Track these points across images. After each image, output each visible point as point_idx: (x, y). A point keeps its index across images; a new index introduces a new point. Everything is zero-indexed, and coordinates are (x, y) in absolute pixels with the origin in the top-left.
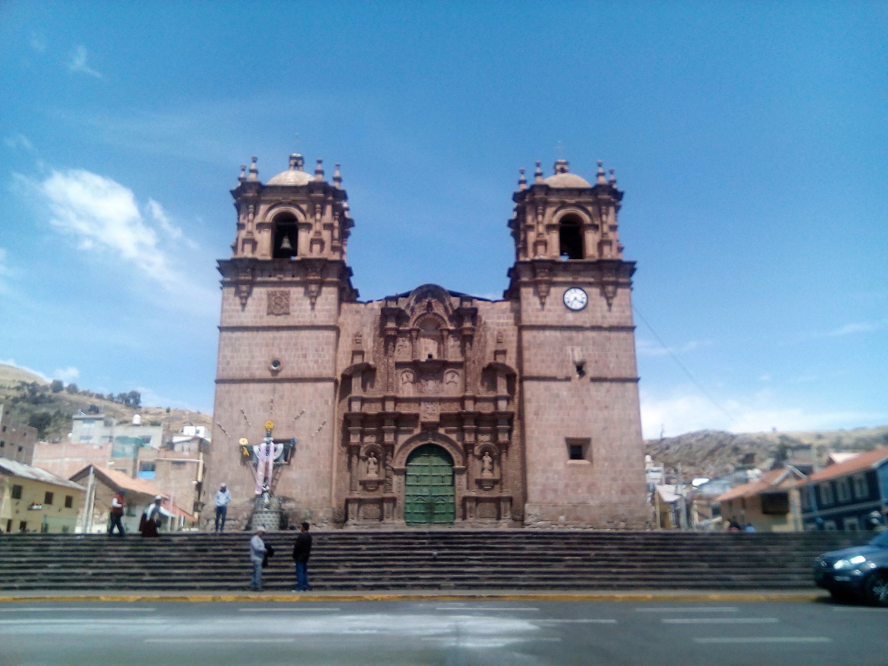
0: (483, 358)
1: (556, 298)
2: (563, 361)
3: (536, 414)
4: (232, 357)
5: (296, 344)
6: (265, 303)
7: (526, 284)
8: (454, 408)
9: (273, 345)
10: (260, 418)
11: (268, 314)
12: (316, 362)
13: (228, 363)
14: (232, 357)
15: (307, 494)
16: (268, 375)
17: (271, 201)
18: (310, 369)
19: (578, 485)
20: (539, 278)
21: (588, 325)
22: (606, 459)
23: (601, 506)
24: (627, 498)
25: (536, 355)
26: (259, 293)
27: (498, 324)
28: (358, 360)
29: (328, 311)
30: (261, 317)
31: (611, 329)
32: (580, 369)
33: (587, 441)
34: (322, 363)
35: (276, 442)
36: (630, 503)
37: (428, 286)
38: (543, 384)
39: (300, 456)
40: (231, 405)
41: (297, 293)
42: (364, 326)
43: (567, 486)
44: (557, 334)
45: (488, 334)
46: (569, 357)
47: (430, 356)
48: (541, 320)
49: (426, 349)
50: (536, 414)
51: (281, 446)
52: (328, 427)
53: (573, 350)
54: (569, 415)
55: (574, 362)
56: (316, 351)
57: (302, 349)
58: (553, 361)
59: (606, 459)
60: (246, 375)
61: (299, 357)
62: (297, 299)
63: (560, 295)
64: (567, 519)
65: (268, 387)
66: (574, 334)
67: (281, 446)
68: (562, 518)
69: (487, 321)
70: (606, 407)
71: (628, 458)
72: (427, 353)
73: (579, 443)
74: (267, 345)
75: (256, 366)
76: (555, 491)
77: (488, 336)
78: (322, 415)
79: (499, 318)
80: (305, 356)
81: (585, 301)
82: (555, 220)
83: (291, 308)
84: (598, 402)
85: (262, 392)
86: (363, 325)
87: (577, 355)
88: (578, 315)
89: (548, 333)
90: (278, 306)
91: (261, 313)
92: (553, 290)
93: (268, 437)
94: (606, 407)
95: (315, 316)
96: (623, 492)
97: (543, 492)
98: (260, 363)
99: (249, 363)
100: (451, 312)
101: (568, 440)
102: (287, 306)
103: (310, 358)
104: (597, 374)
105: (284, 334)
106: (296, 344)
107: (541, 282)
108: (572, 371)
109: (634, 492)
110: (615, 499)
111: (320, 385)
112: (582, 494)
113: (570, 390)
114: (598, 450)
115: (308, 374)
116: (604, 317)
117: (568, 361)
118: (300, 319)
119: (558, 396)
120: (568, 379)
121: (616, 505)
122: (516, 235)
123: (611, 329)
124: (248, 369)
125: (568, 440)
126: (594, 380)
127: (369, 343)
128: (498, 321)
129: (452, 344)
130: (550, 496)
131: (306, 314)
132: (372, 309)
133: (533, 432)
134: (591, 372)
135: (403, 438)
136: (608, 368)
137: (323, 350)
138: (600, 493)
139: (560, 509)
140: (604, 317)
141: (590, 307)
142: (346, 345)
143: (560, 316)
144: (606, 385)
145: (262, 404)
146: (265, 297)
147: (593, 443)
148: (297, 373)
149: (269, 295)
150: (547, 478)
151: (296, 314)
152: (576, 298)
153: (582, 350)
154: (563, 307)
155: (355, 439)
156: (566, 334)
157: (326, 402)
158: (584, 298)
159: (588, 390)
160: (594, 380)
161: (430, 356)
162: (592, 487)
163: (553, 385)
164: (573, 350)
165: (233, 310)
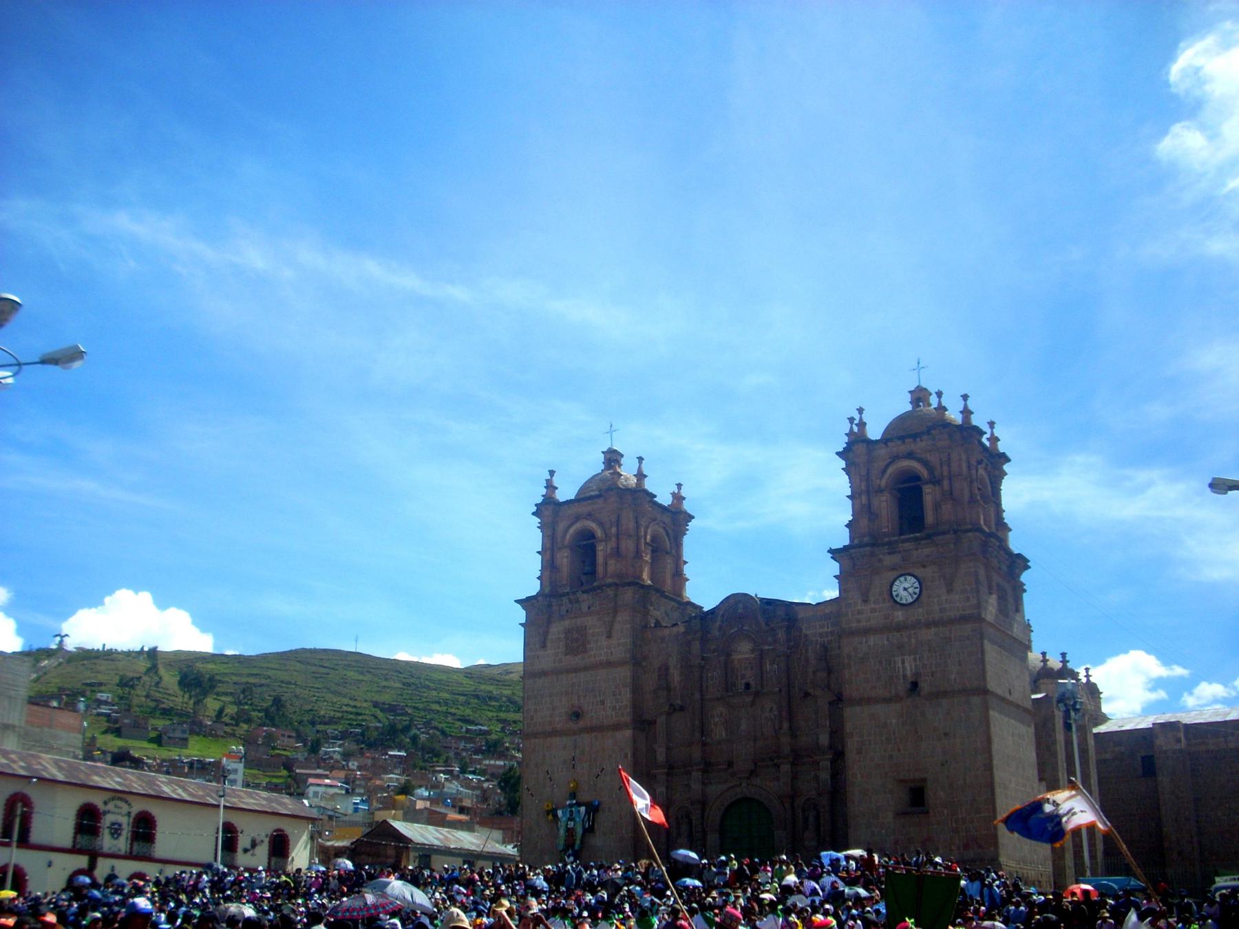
3: (859, 752)
4: (536, 711)
9: (572, 693)
11: (566, 655)
12: (614, 708)
13: (532, 719)
14: (536, 711)
27: (821, 635)
31: (952, 621)
33: (924, 780)
34: (619, 709)
42: (670, 656)
43: (896, 842)
45: (810, 648)
46: (899, 672)
47: (748, 686)
49: (743, 677)
50: (859, 752)
51: (583, 809)
53: (903, 663)
54: (899, 750)
56: (614, 695)
57: (600, 696)
61: (597, 705)
67: (583, 809)
69: (808, 632)
72: (744, 682)
75: (557, 719)
79: (822, 627)
80: (603, 702)
81: (917, 591)
83: (588, 646)
87: (908, 666)
89: (872, 640)
91: (560, 657)
93: (570, 799)
94: (946, 734)
95: (611, 653)
96: (966, 847)
108: (902, 687)
109: (980, 847)
114: (936, 795)
116: (942, 610)
118: (596, 658)
120: (897, 699)
128: (821, 630)
131: (602, 652)
134: (925, 687)
137: (620, 694)
140: (942, 610)
141: (924, 599)
146: (562, 636)
152: (905, 588)
153: (915, 660)
158: (917, 588)
163: (879, 709)
164: (903, 663)
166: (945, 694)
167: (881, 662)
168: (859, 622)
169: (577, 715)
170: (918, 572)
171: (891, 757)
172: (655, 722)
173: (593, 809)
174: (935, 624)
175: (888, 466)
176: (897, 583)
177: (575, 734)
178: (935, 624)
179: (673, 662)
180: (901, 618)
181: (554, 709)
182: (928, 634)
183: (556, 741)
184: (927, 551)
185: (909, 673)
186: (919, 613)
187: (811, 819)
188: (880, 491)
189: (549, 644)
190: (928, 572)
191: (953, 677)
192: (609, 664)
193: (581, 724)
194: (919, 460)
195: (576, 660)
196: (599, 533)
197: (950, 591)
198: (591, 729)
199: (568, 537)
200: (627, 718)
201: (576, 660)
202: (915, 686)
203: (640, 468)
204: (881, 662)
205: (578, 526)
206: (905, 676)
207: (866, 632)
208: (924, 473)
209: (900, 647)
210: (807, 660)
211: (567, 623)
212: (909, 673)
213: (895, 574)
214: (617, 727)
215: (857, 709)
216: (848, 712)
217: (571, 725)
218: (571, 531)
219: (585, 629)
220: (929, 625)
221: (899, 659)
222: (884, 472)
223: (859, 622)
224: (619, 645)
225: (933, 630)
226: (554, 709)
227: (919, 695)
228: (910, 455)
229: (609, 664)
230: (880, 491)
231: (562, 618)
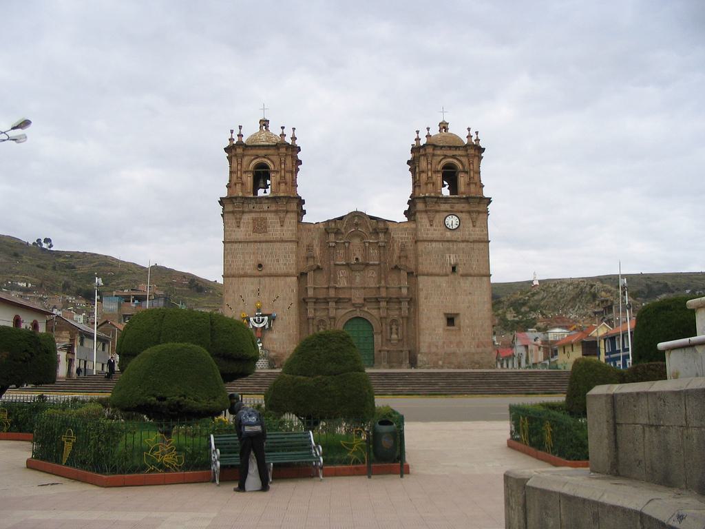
0: (392, 261)
1: (439, 222)
2: (443, 264)
5: (272, 253)
6: (251, 226)
7: (421, 212)
8: (372, 294)
9: (257, 253)
10: (251, 300)
13: (230, 265)
15: (283, 348)
16: (256, 272)
17: (252, 155)
18: (281, 268)
19: (451, 343)
20: (428, 208)
21: (460, 239)
22: (468, 327)
23: (465, 355)
24: (480, 350)
25: (426, 260)
26: (247, 218)
28: (311, 263)
29: (291, 231)
30: (250, 235)
31: (474, 242)
32: (454, 269)
33: (457, 315)
35: (262, 315)
36: (482, 353)
37: (357, 212)
38: (431, 278)
39: (278, 325)
40: (234, 292)
41: (271, 218)
42: (314, 239)
43: (444, 343)
44: (439, 245)
48: (430, 236)
49: (355, 255)
51: (266, 318)
52: (294, 306)
53: (450, 257)
55: (450, 264)
58: (437, 263)
59: (468, 327)
60: (242, 272)
62: (271, 223)
63: (442, 220)
64: (443, 363)
65: (256, 280)
66: (451, 245)
67: (266, 318)
68: (440, 363)
69: (394, 236)
70: (470, 293)
71: (482, 325)
72: (355, 257)
73: (453, 316)
74: (254, 253)
75: (247, 267)
76: (437, 346)
77: (396, 247)
78: (290, 299)
79: (402, 234)
82: (439, 167)
84: (465, 291)
85: (252, 284)
86: (313, 239)
87: (453, 260)
88: (455, 232)
89: (434, 244)
90: (260, 226)
92: (438, 216)
94: (470, 293)
96: (478, 347)
97: (429, 347)
98: (249, 265)
99: (243, 265)
100: (371, 230)
101: (445, 314)
102: (266, 227)
103: (281, 262)
104: (465, 272)
105: (264, 245)
106: (272, 253)
107: (429, 211)
110: (473, 350)
111: (288, 279)
112: (453, 348)
113: (448, 282)
114: (463, 321)
115: (279, 272)
116: (470, 235)
117: (447, 264)
119: (440, 286)
120: (446, 275)
121: (473, 354)
122: (413, 170)
123: (474, 242)
124: (243, 269)
125: (445, 314)
126: (462, 276)
127: (317, 251)
129: (374, 252)
130: (434, 350)
132: (319, 228)
133: (423, 310)
134: (460, 270)
135: (342, 312)
136: (472, 268)
138: (464, 347)
139: (439, 357)
141: (461, 227)
142: (304, 253)
143: (442, 234)
144: (470, 278)
145: (253, 291)
147: (461, 316)
148: (273, 271)
149: (254, 220)
150: (432, 339)
151: (271, 233)
152: (452, 221)
154: (445, 227)
155: (311, 313)
156: (446, 244)
157: (293, 291)
159: (459, 283)
160: (462, 275)
161: (357, 259)
162: (459, 343)
164: (450, 257)
165: (231, 231)
166: (471, 275)
167: (438, 256)
168: (427, 234)
169: (260, 266)
170: (458, 214)
171: (442, 302)
172: (307, 274)
173: (272, 319)
174: (468, 241)
175: (441, 160)
176: (448, 218)
177: (260, 276)
178: (468, 241)
179: (316, 242)
180: (449, 235)
181: (245, 262)
182: (463, 245)
183: (245, 279)
184: (463, 205)
185: (452, 262)
186: (458, 235)
187: (394, 330)
188: (438, 171)
189: (242, 225)
190: (463, 216)
191: (474, 267)
192: (282, 241)
193: (264, 272)
194: (458, 159)
195: (261, 237)
196: (272, 167)
197: (474, 226)
198: (270, 276)
199: (251, 165)
200: (293, 270)
201: (261, 237)
202: (454, 269)
203: (294, 134)
204: (438, 256)
205: (258, 160)
206: (450, 264)
207: (431, 241)
208: (460, 167)
209: (448, 249)
210: (394, 250)
211: (253, 215)
212: (452, 262)
213: (447, 214)
214: (286, 275)
215: (426, 277)
216: (422, 280)
217: (256, 272)
218: (254, 162)
219: (266, 219)
220: (463, 241)
221: (448, 256)
222: (440, 162)
223: (427, 234)
224: (288, 230)
225: (465, 244)
226: (245, 262)
227: (458, 274)
228: (454, 157)
229: (282, 241)
230: (438, 171)
231: (250, 212)
